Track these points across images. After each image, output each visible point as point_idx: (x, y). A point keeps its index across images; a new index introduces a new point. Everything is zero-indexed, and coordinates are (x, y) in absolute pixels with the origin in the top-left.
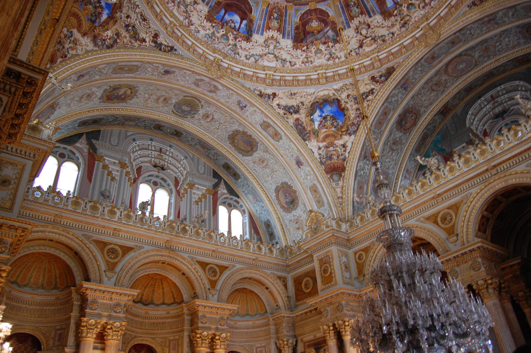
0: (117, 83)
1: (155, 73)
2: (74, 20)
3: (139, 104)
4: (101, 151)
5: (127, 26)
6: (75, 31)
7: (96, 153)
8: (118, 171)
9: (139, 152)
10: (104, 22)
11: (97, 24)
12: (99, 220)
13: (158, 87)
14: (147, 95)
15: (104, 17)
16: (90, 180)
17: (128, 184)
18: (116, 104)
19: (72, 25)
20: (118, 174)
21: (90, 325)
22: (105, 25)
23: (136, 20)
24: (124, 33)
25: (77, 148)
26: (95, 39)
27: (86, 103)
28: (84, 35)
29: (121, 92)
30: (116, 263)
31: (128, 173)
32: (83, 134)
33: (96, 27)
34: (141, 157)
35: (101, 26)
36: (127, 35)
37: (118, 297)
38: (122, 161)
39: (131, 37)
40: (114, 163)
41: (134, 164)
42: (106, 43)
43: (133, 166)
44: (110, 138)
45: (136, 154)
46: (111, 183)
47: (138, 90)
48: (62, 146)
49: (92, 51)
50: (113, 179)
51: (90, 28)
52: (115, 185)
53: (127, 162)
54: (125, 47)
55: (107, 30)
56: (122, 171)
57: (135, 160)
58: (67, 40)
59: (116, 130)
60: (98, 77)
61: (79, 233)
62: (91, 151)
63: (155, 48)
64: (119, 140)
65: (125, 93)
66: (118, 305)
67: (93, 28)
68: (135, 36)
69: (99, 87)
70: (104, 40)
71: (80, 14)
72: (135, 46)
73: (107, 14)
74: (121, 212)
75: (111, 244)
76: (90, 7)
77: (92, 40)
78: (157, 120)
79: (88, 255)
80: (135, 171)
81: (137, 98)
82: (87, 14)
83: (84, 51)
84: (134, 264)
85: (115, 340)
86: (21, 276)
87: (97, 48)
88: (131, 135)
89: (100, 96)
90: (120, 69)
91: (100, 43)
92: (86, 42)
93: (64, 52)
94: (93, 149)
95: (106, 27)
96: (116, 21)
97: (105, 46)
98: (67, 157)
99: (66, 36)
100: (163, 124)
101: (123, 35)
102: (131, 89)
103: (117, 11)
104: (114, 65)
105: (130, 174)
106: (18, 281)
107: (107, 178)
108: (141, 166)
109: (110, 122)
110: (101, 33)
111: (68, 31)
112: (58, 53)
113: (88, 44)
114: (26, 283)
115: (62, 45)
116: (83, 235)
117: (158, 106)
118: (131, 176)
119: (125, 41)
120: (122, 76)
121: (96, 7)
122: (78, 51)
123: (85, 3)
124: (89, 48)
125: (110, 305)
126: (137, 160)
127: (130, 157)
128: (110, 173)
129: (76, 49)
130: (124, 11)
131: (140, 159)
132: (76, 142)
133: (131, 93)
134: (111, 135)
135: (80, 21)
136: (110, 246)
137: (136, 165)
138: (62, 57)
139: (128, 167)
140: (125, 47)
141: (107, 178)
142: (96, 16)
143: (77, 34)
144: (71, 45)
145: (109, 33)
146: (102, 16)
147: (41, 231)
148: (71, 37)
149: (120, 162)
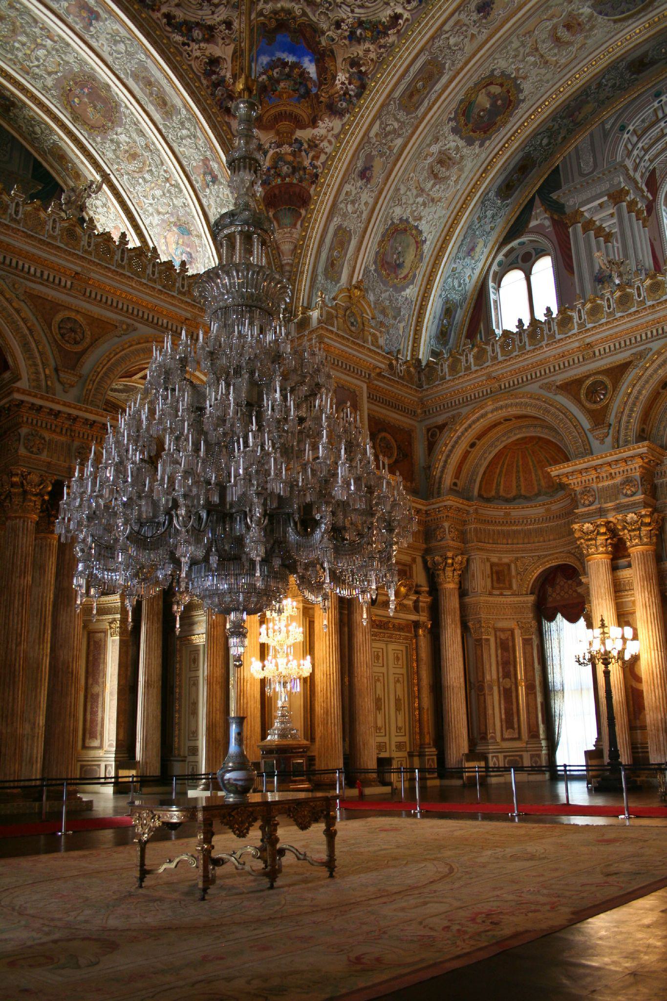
0: (454, 105)
1: (474, 31)
2: (284, 125)
3: (545, 79)
4: (571, 203)
5: (352, 36)
6: (299, 134)
7: (565, 213)
8: (612, 215)
9: (640, 145)
10: (319, 74)
11: (314, 90)
12: (546, 349)
13: (521, 31)
14: (532, 59)
15: (311, 69)
16: (572, 272)
17: (637, 225)
18: (513, 120)
19: (287, 133)
20: (615, 220)
21: (587, 534)
22: (326, 76)
23: (352, 11)
24: (358, 50)
25: (532, 232)
26: (333, 111)
27: (461, 170)
28: (314, 123)
29: (483, 101)
30: (607, 405)
31: (632, 205)
32: (533, 197)
33: (316, 94)
34: (646, 151)
35: (321, 84)
36: (367, 45)
37: (622, 467)
38: (612, 191)
39: (374, 40)
40: (601, 206)
41: (638, 176)
42: (351, 93)
43: (636, 183)
44: (579, 164)
45: (635, 152)
46: (606, 247)
47: (503, 72)
48: (514, 244)
49: (343, 125)
50: (608, 237)
51: (313, 108)
52: (617, 244)
53: (623, 185)
54: (381, 63)
55: (334, 77)
56: (619, 211)
57: (635, 170)
58: (300, 156)
59: (581, 139)
60: (399, 142)
61: (534, 388)
62: (556, 217)
63: (424, 5)
64: (595, 157)
65: (494, 98)
66: (628, 481)
67: (315, 101)
68: (377, 30)
69: (436, 140)
70: (345, 94)
71: (283, 108)
72: (393, 44)
73: (311, 61)
74: (579, 311)
75: (588, 377)
76: (282, 85)
77: (330, 117)
78: (621, 58)
79: (557, 417)
80: (645, 189)
81: (525, 78)
82: (289, 97)
83: (333, 140)
84: (640, 392)
85: (637, 545)
86: (522, 484)
87: (347, 116)
88: (613, 124)
89: (461, 143)
90: (411, 95)
91: (344, 104)
92: (327, 126)
93: (309, 174)
94: (556, 209)
95: (329, 76)
96: (332, 51)
97: (354, 100)
98: (534, 254)
99: (294, 154)
100: (639, 53)
101: (361, 54)
102: (491, 83)
103: (317, 40)
104: (392, 107)
105: (637, 203)
106: (523, 492)
107: (598, 243)
108: (655, 169)
109: (549, 144)
110: (332, 91)
111: (291, 146)
112: (304, 184)
113: (331, 125)
114: (536, 490)
115: (300, 169)
116: (540, 388)
117: (576, 46)
118: (639, 206)
119: (372, 55)
120: (434, 96)
121: (289, 76)
122: (327, 150)
123: (272, 90)
124: (336, 131)
125: (615, 486)
126: (642, 164)
127: (627, 170)
128: (599, 231)
129: (322, 151)
130: (325, 27)
131: (647, 157)
132: (528, 221)
133: (501, 85)
134: (578, 158)
135: (291, 115)
136: (589, 382)
137: (642, 177)
138: (313, 182)
139: (628, 193)
140: (380, 63)
141: (598, 243)
142: (301, 83)
143: (303, 134)
144: (311, 155)
145: (341, 77)
146: (309, 73)
147: (482, 416)
148: (302, 145)
149: (610, 196)
